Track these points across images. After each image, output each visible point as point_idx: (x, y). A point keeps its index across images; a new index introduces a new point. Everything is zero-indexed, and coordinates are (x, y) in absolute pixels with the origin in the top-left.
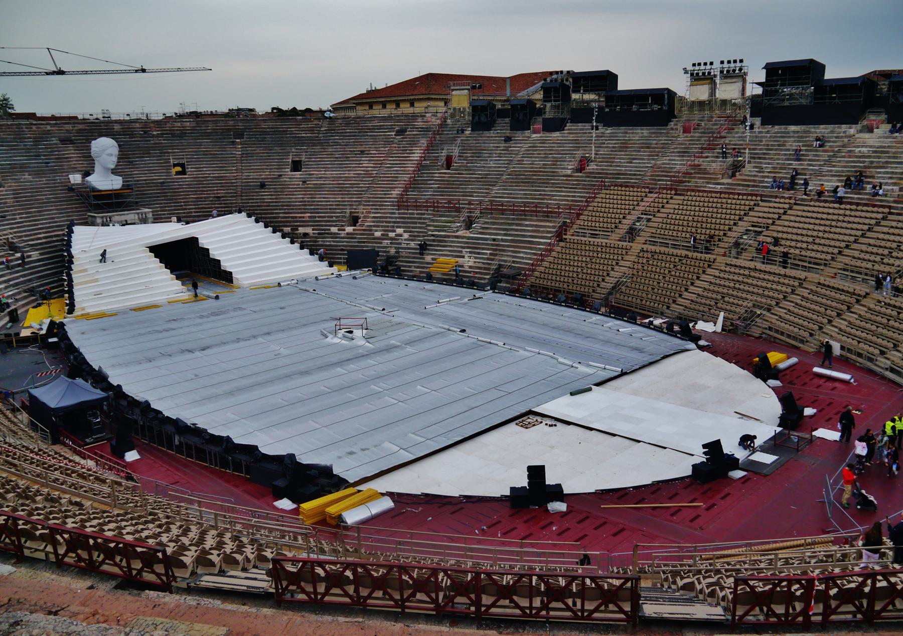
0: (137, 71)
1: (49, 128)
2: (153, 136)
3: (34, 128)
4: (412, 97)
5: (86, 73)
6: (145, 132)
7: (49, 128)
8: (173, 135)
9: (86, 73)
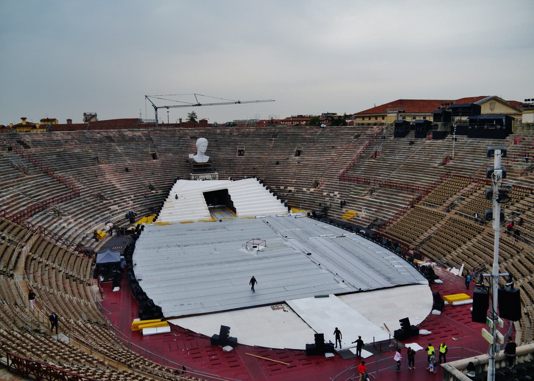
0: (236, 103)
1: (188, 131)
2: (234, 136)
4: (383, 114)
5: (211, 104)
6: (231, 134)
7: (188, 131)
8: (243, 135)
9: (211, 104)
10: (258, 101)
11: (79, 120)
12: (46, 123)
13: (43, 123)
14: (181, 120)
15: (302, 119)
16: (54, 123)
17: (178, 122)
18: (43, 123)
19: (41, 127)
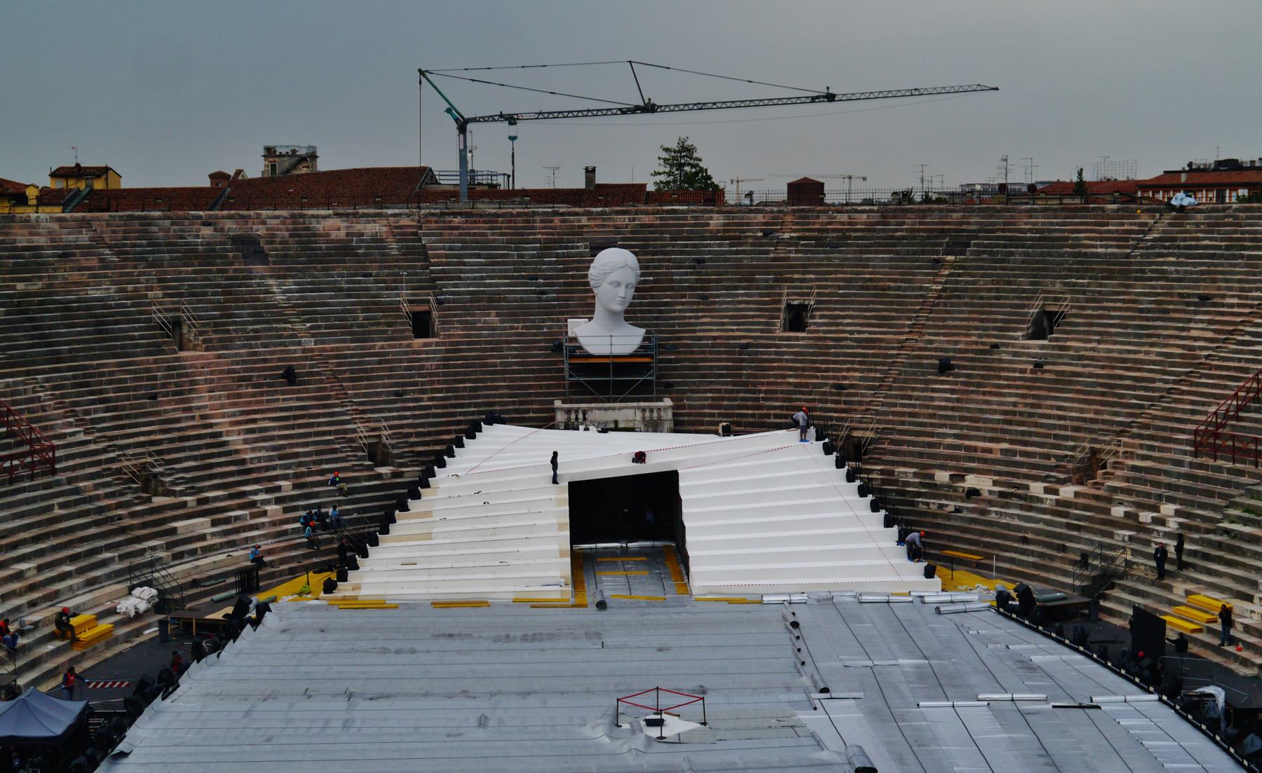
0: (813, 99)
1: (584, 221)
2: (780, 242)
3: (557, 221)
5: (701, 106)
7: (584, 221)
8: (820, 242)
9: (701, 106)
10: (915, 92)
11: (255, 169)
12: (72, 184)
13: (59, 184)
14: (590, 172)
15: (1235, 177)
16: (98, 185)
17: (580, 184)
18: (59, 184)
19: (47, 198)
